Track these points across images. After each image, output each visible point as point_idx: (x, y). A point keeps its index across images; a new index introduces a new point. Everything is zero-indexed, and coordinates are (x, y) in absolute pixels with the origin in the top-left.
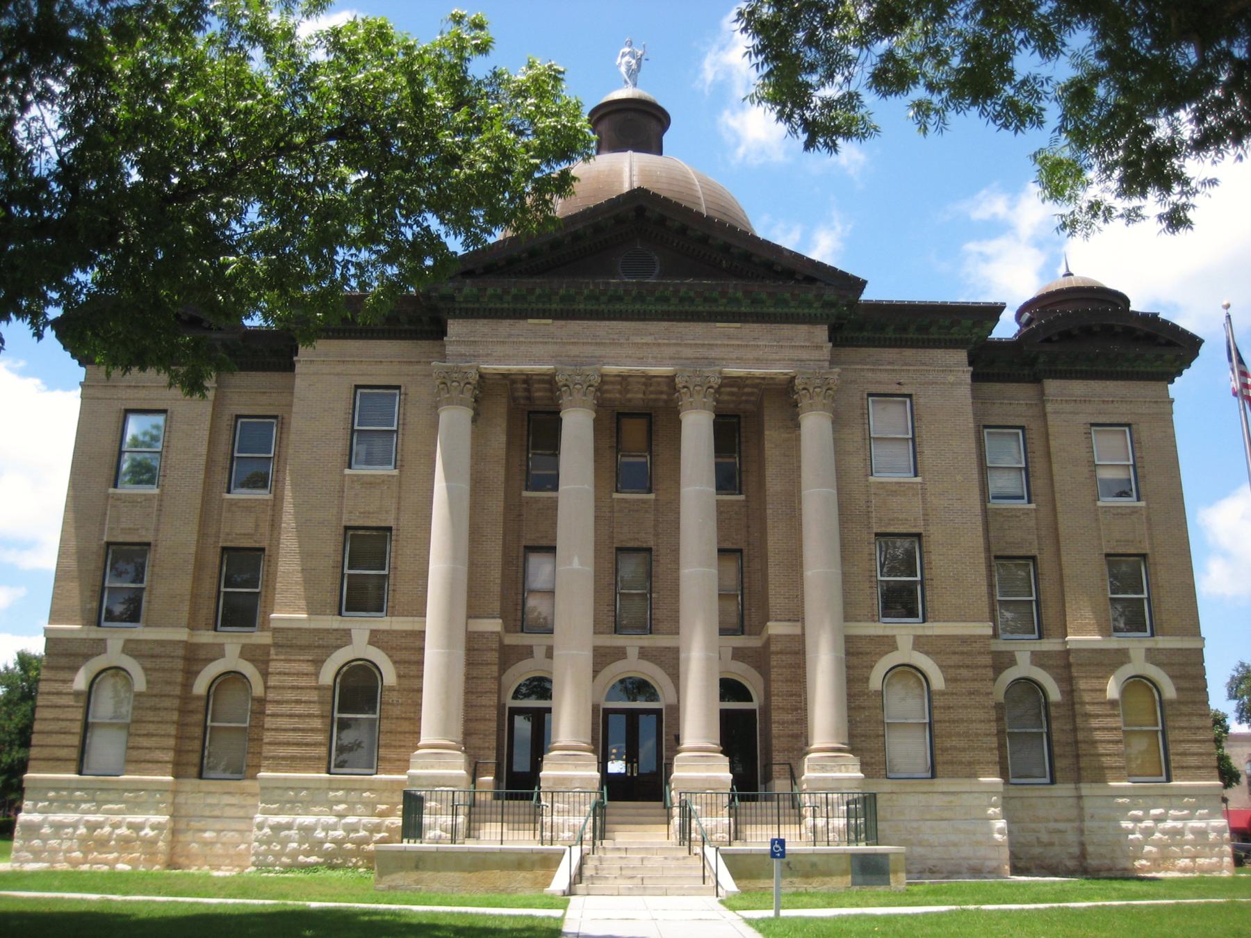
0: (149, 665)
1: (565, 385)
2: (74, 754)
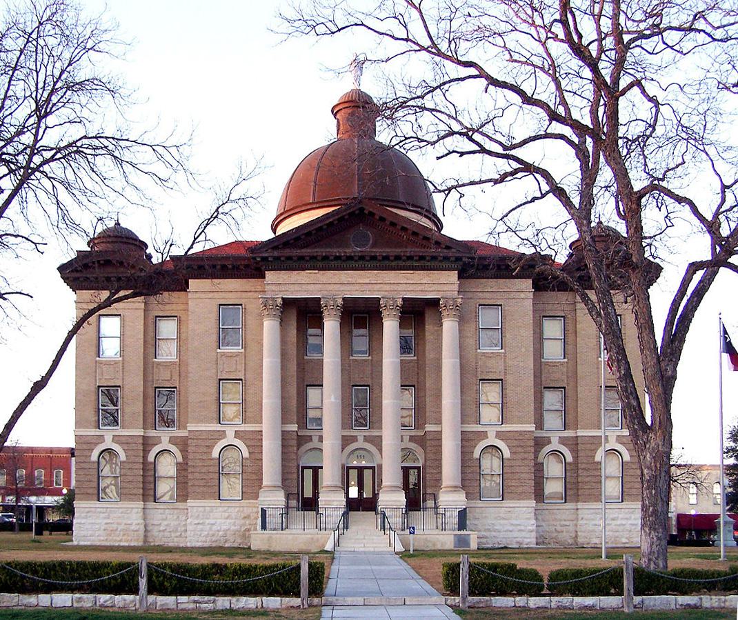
0: (126, 448)
1: (325, 306)
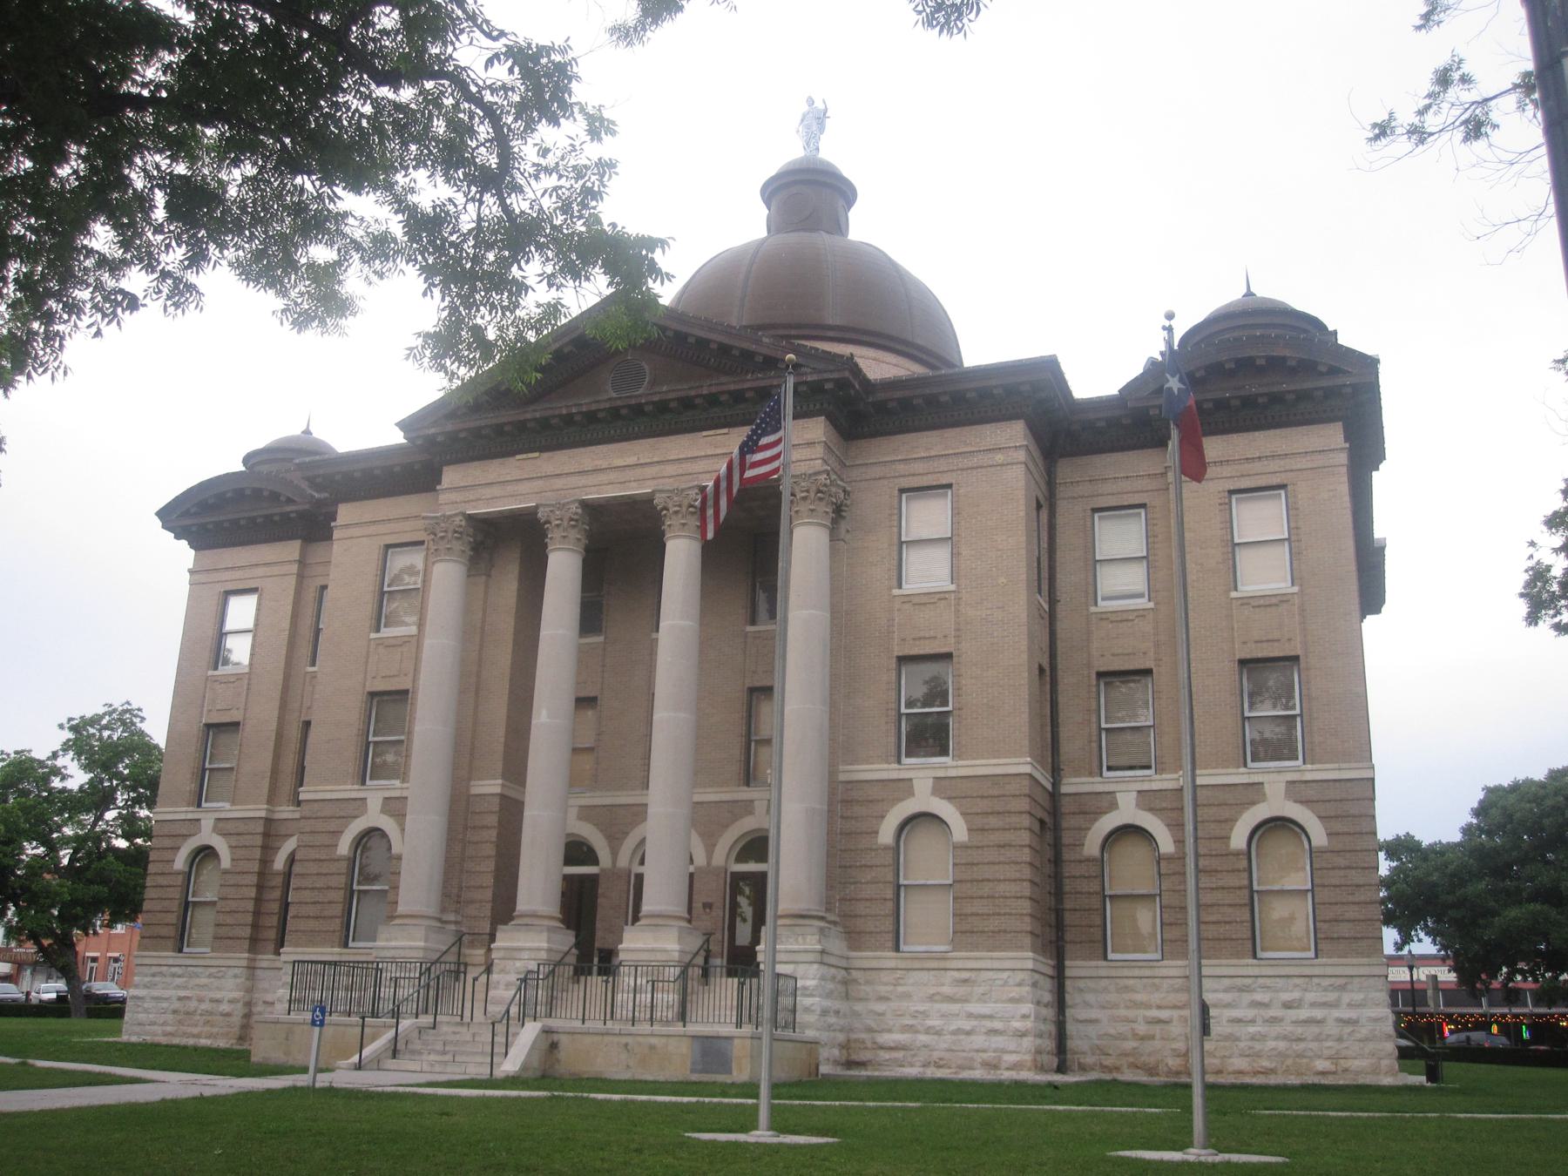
2: (336, 924)
